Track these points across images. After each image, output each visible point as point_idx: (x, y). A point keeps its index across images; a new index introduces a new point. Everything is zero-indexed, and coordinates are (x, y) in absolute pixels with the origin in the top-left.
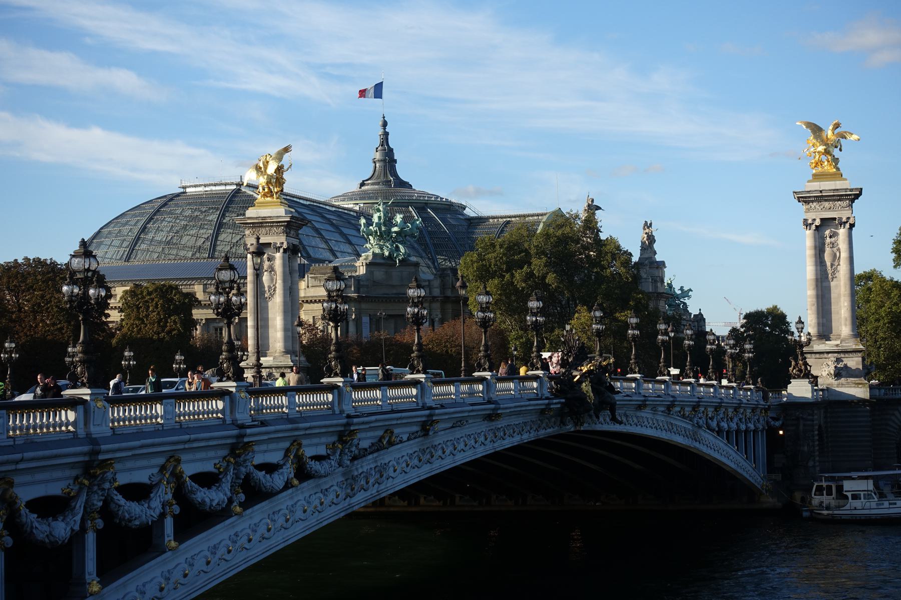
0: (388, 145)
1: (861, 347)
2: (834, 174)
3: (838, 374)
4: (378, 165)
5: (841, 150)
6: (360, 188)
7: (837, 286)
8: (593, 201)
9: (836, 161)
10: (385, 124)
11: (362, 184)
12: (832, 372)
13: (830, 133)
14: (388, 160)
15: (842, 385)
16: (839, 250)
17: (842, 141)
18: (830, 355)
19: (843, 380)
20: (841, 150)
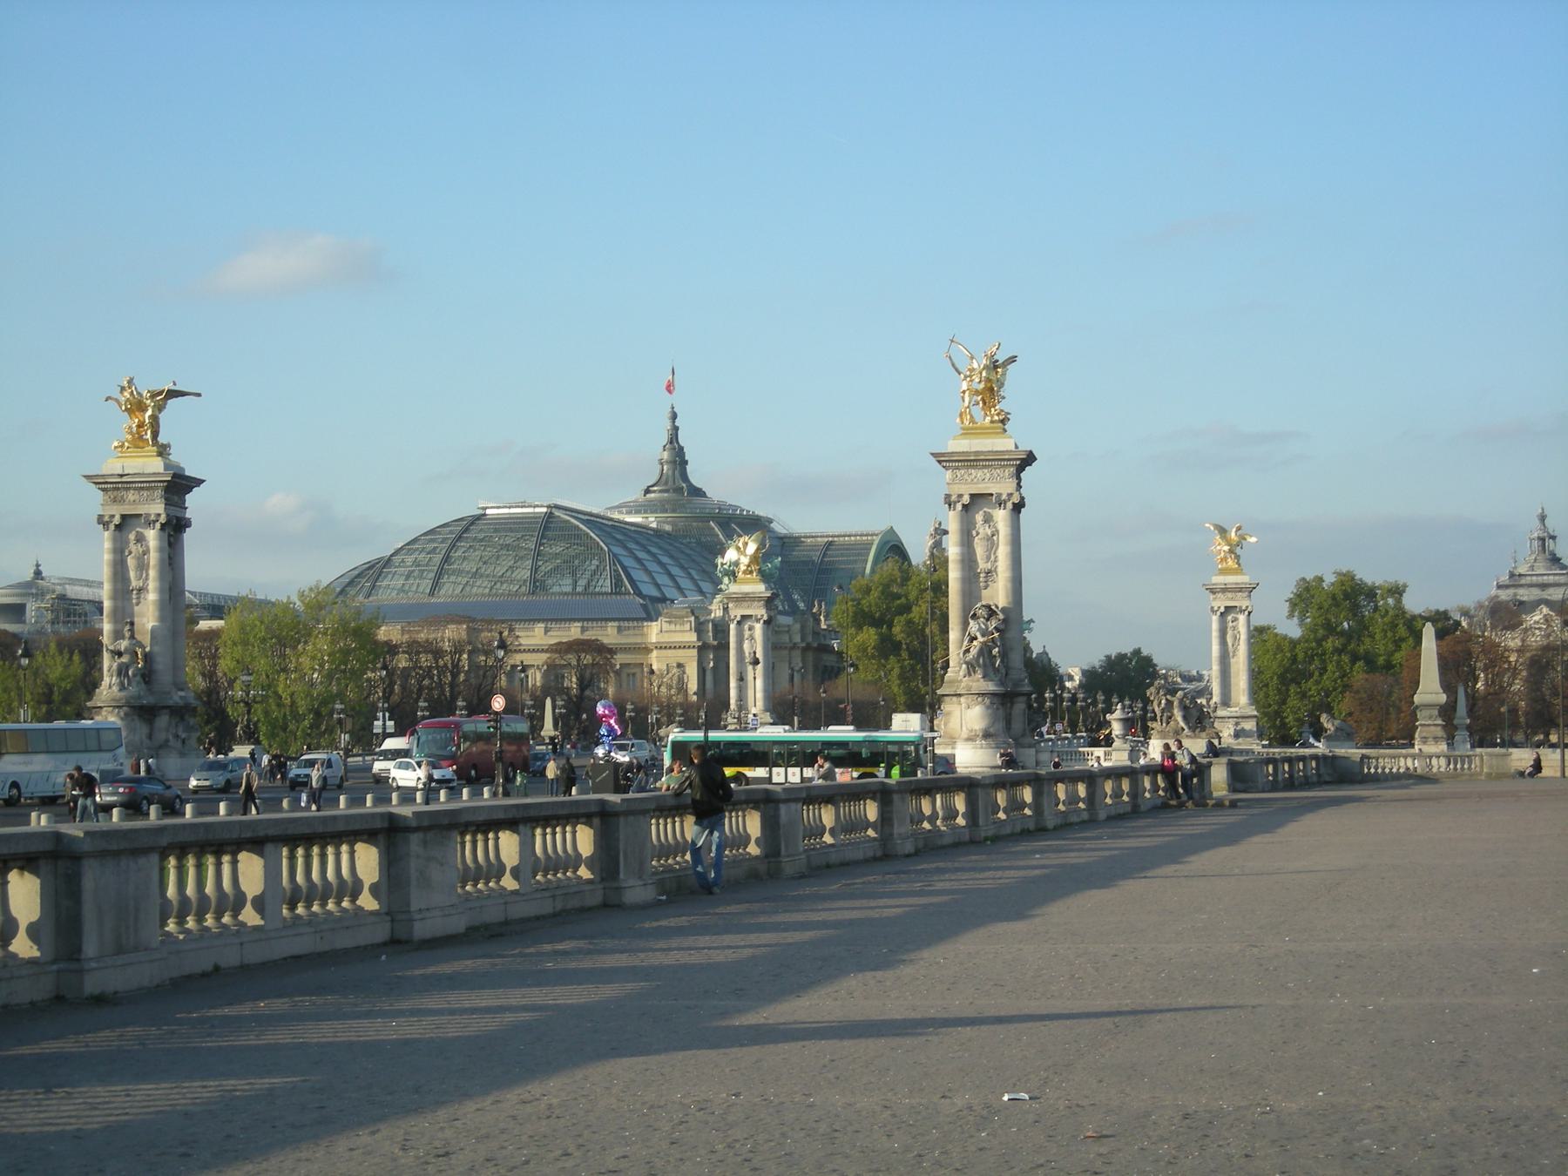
0: (678, 443)
1: (1255, 713)
2: (1236, 569)
3: (1237, 735)
4: (665, 467)
5: (1242, 548)
6: (645, 496)
7: (1237, 663)
8: (940, 524)
9: (1238, 557)
10: (674, 416)
11: (647, 491)
12: (1232, 734)
13: (1233, 534)
14: (679, 459)
15: (1239, 744)
16: (1239, 632)
17: (1243, 542)
18: (1230, 720)
19: (1240, 740)
20: (1242, 548)
